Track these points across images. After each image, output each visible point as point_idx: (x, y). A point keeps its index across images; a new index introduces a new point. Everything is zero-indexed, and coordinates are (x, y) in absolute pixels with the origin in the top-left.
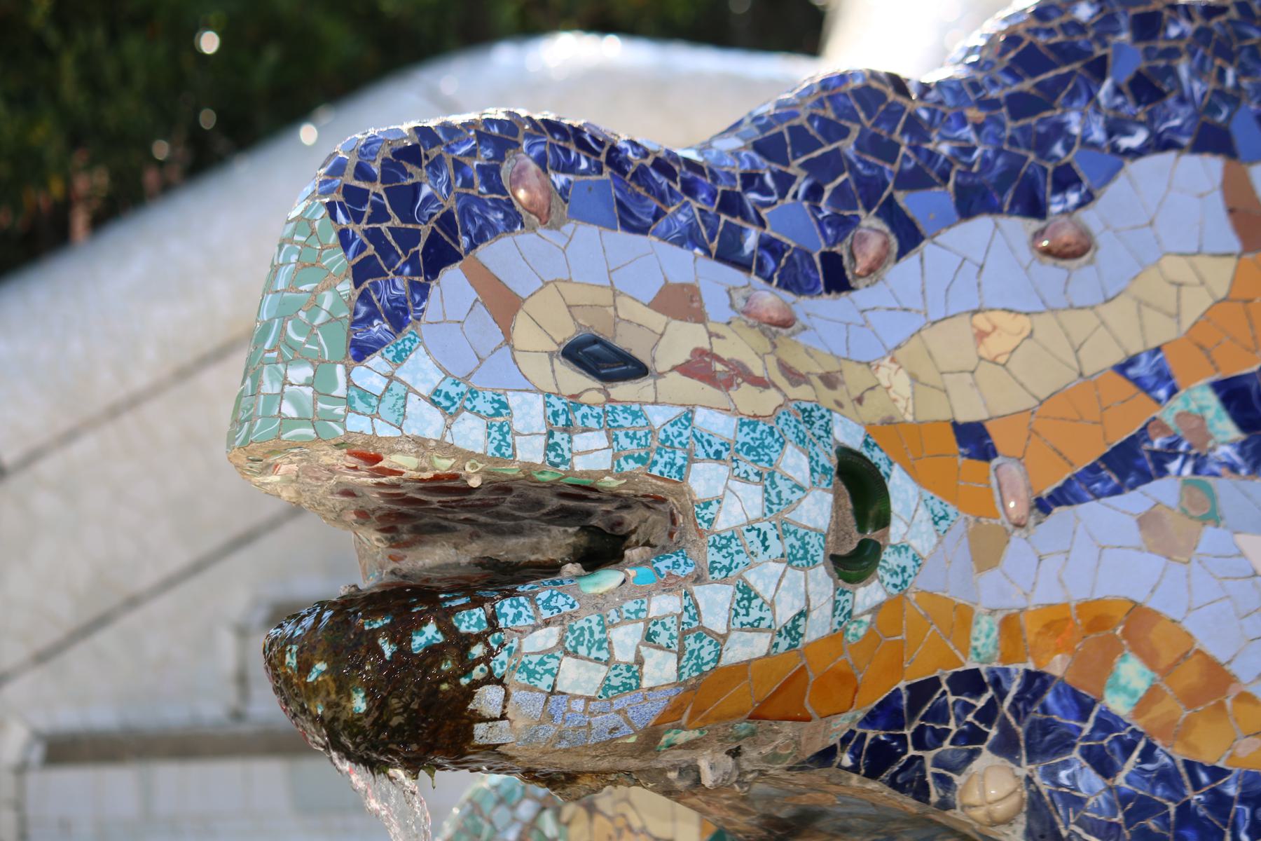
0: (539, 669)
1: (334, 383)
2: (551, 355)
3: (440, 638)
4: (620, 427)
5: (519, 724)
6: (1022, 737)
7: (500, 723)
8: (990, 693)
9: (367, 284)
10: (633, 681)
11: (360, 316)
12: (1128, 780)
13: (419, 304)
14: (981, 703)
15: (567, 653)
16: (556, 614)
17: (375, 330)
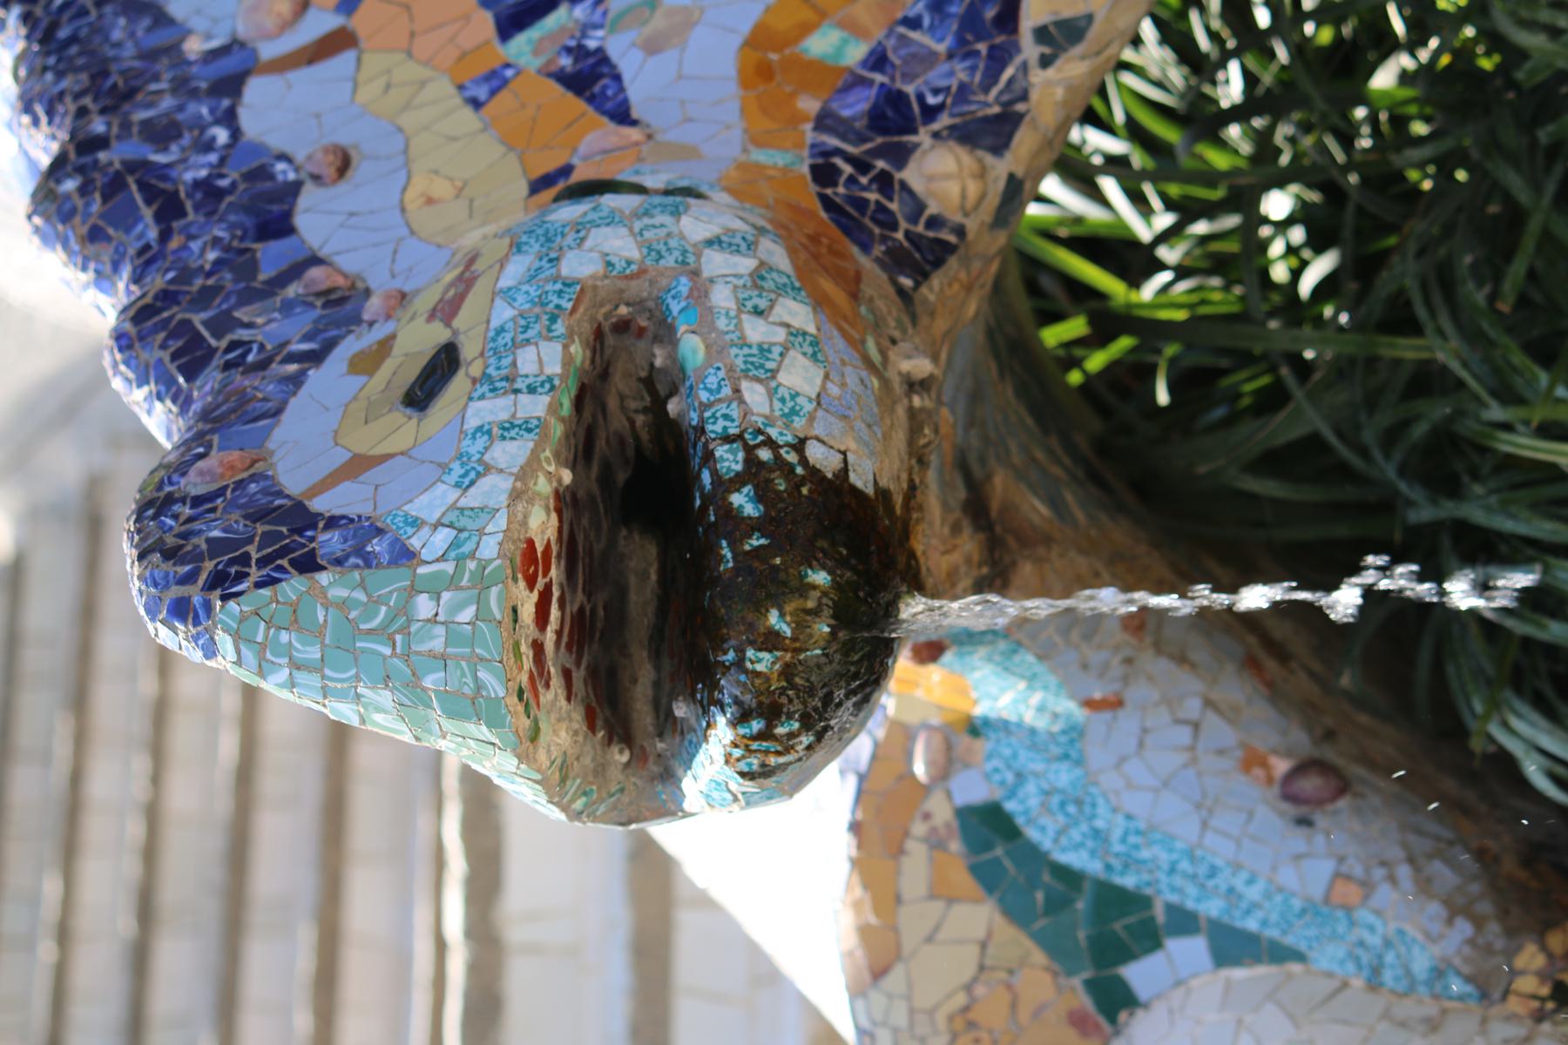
0: (790, 404)
2: (420, 420)
3: (746, 490)
5: (852, 445)
7: (851, 457)
8: (838, 161)
9: (324, 563)
11: (360, 562)
12: (941, 40)
13: (352, 521)
14: (848, 169)
15: (774, 377)
17: (377, 549)
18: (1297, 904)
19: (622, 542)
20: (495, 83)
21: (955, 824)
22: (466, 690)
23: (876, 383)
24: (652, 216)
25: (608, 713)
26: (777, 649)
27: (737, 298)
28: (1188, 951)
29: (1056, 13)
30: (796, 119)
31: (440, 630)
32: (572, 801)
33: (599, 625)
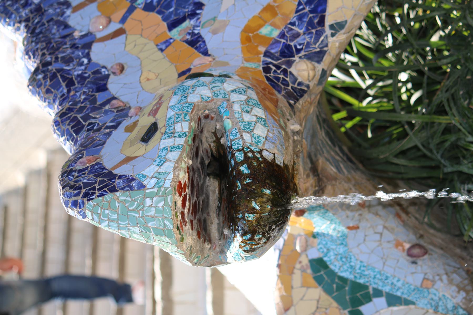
2: (146, 146)
3: (244, 165)
6: (286, 59)
7: (276, 155)
9: (118, 189)
11: (129, 189)
12: (301, 29)
13: (126, 176)
14: (274, 68)
15: (252, 131)
18: (412, 287)
19: (207, 181)
20: (167, 44)
21: (309, 265)
22: (161, 227)
23: (283, 133)
25: (204, 233)
26: (255, 213)
28: (380, 302)
29: (336, 20)
30: (259, 53)
31: (153, 209)
32: (194, 260)
33: (201, 207)
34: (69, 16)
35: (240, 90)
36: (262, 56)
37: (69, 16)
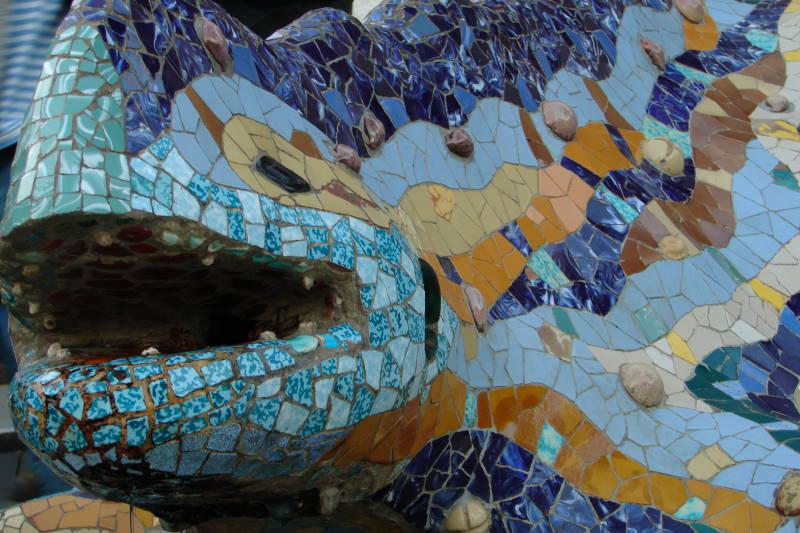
0: (267, 412)
1: (120, 171)
4: (308, 225)
8: (472, 450)
10: (321, 424)
11: (130, 118)
13: (166, 116)
14: (467, 457)
15: (286, 400)
16: (280, 367)
17: (142, 130)
20: (518, 242)
24: (406, 319)
27: (346, 374)
31: (75, 170)
34: (577, 72)
35: (392, 373)
36: (494, 429)
37: (577, 72)
